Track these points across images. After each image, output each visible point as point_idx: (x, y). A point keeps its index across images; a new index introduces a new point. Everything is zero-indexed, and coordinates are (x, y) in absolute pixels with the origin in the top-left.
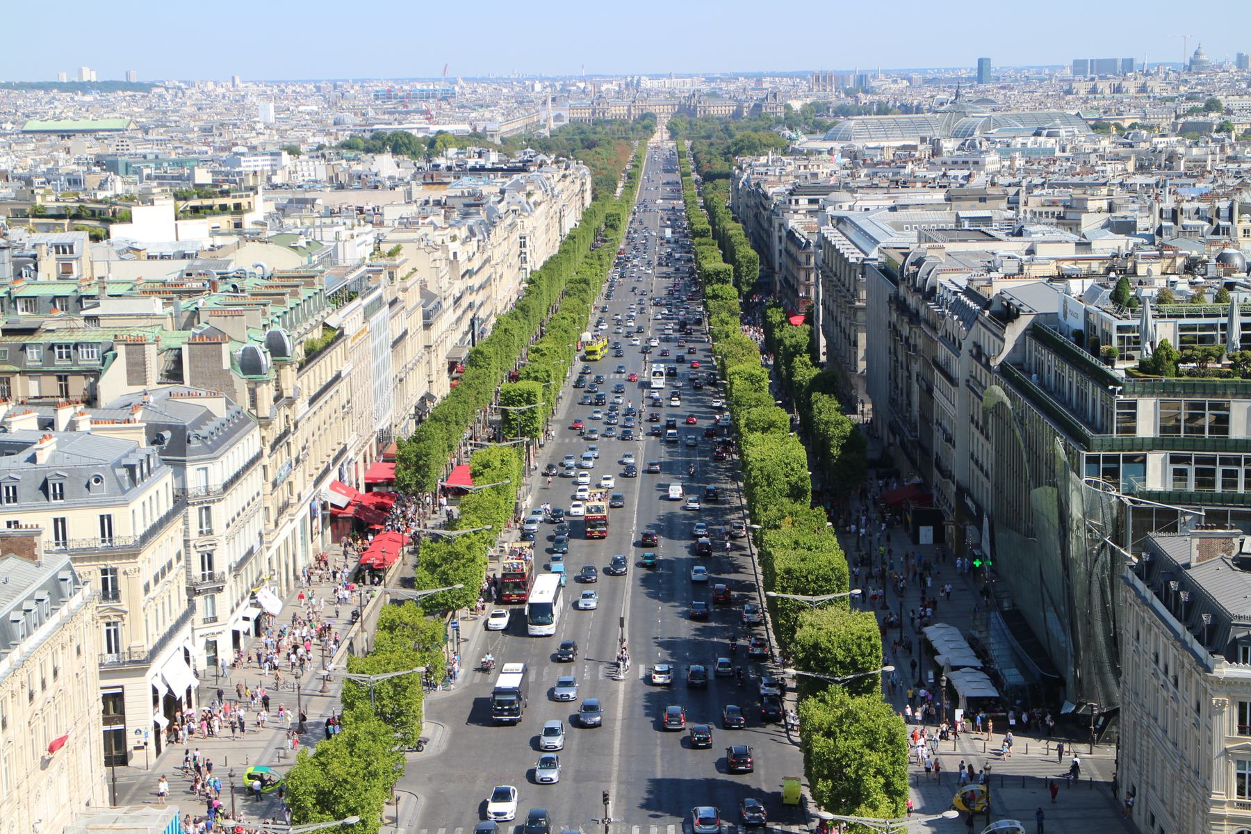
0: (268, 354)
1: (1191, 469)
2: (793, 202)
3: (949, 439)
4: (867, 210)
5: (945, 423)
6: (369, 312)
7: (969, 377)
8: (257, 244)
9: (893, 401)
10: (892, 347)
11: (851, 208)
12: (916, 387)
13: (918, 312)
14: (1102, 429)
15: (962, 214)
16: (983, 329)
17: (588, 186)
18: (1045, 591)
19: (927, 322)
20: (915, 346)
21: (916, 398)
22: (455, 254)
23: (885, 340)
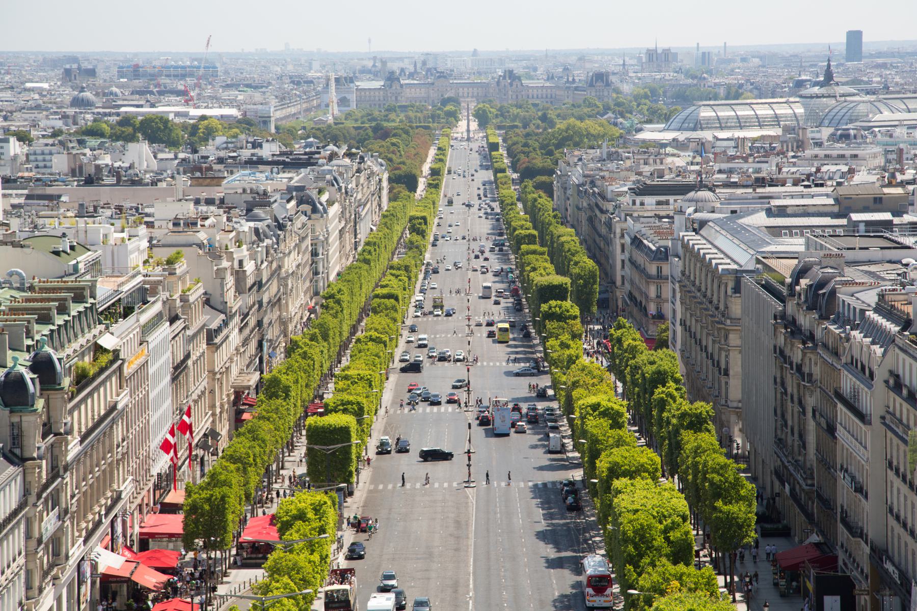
0: (37, 381)
2: (638, 202)
4: (734, 212)
5: (852, 469)
6: (148, 328)
8: (10, 247)
10: (778, 376)
12: (811, 425)
15: (855, 217)
16: (902, 355)
17: (385, 184)
19: (825, 346)
20: (810, 375)
21: (811, 439)
22: (241, 263)
23: (768, 368)
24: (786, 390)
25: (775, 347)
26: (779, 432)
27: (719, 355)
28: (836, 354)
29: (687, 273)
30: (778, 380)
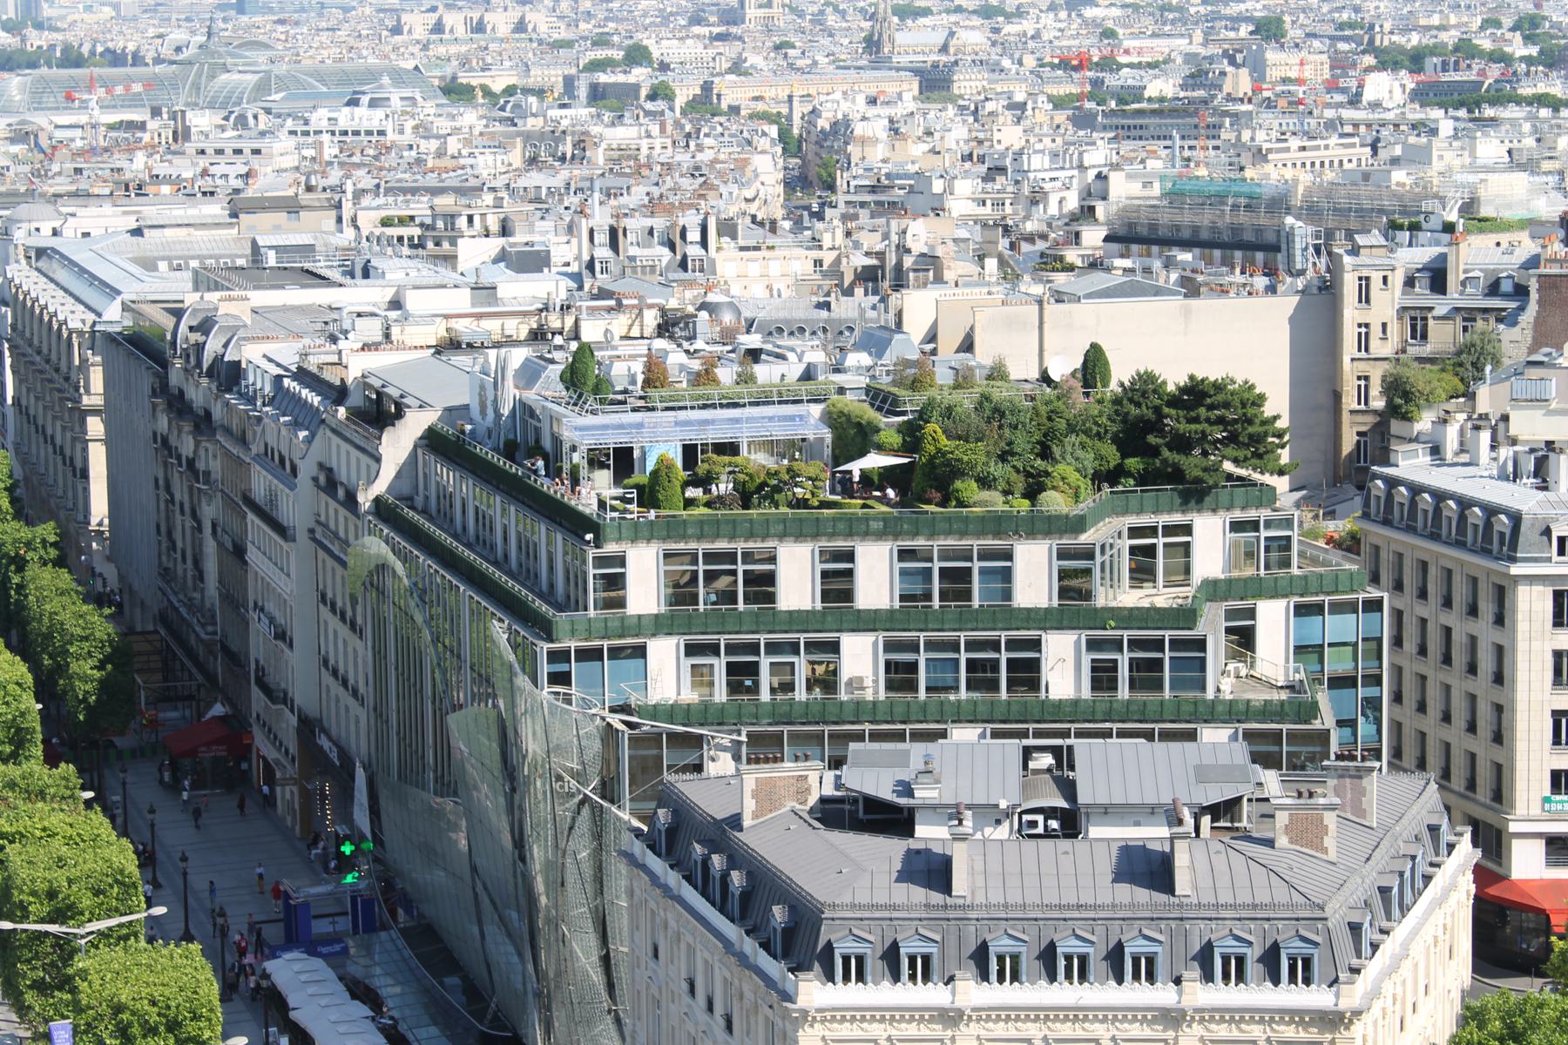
1: (720, 664)
3: (281, 635)
4: (86, 235)
5: (270, 607)
7: (312, 525)
9: (166, 574)
11: (55, 233)
12: (210, 547)
13: (208, 414)
14: (574, 602)
16: (336, 440)
18: (479, 888)
19: (228, 431)
20: (207, 474)
21: (211, 567)
23: (148, 467)
24: (172, 496)
25: (155, 434)
26: (164, 558)
27: (73, 448)
28: (243, 441)
29: (20, 326)
30: (161, 482)
